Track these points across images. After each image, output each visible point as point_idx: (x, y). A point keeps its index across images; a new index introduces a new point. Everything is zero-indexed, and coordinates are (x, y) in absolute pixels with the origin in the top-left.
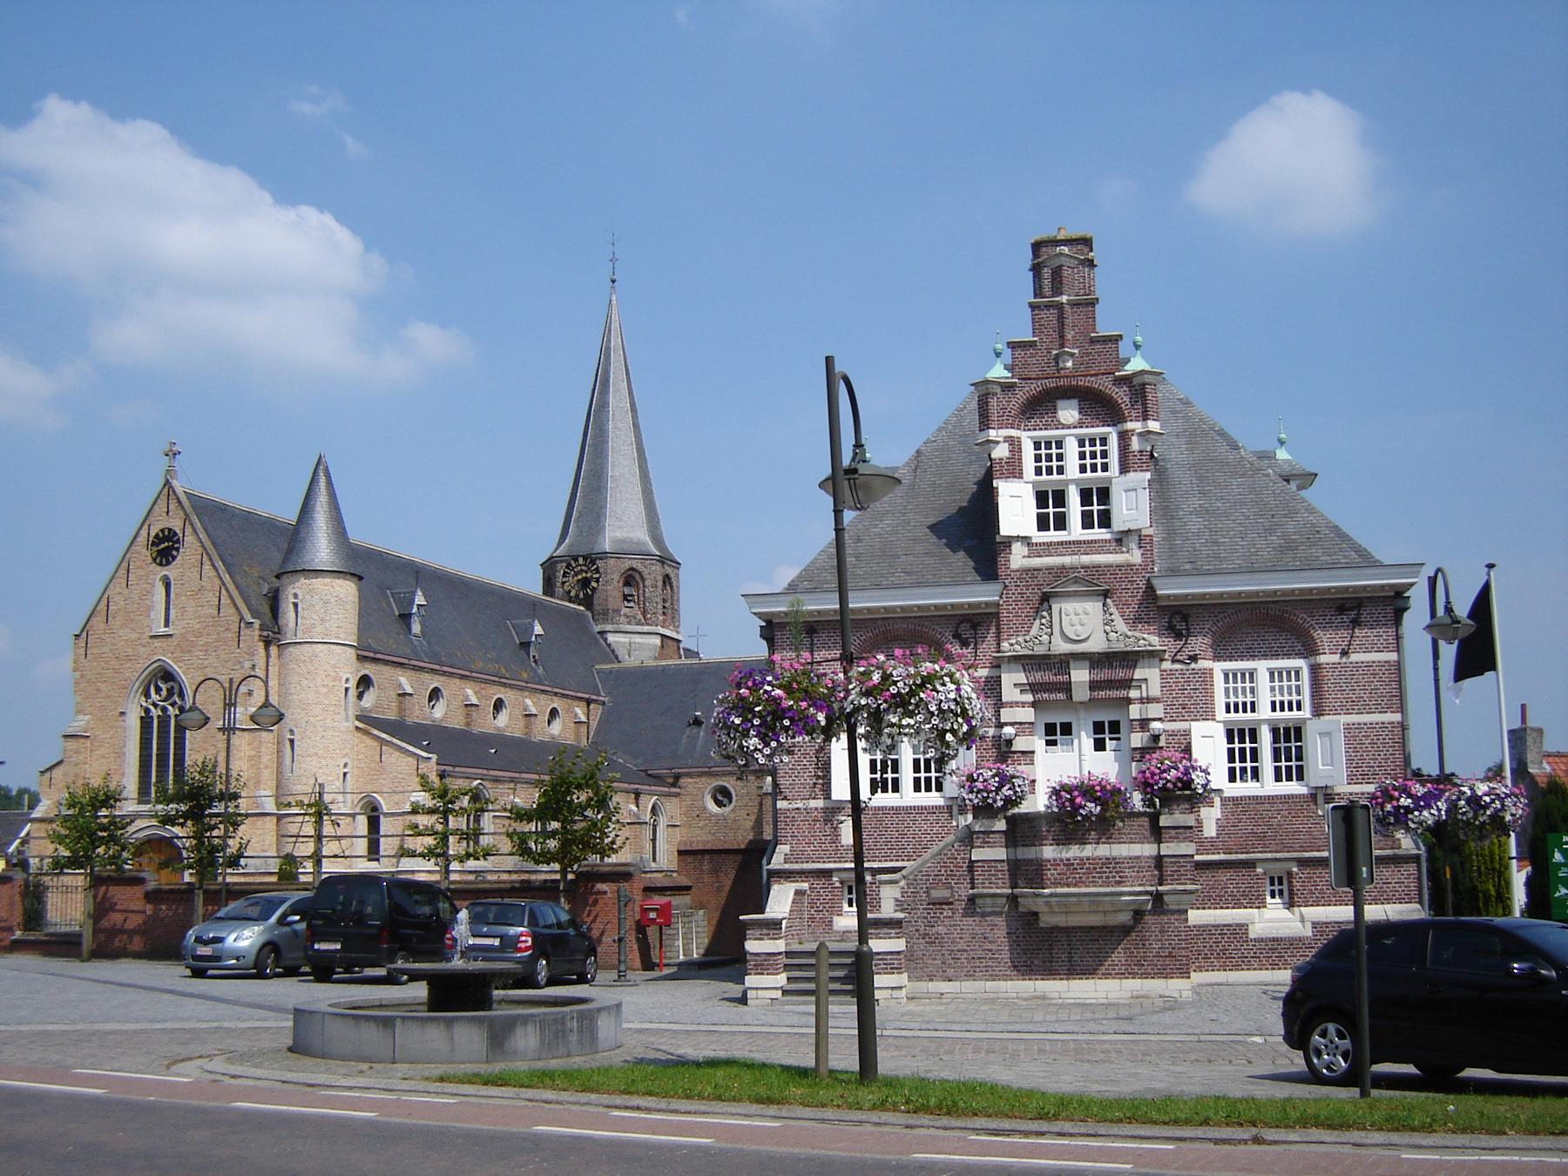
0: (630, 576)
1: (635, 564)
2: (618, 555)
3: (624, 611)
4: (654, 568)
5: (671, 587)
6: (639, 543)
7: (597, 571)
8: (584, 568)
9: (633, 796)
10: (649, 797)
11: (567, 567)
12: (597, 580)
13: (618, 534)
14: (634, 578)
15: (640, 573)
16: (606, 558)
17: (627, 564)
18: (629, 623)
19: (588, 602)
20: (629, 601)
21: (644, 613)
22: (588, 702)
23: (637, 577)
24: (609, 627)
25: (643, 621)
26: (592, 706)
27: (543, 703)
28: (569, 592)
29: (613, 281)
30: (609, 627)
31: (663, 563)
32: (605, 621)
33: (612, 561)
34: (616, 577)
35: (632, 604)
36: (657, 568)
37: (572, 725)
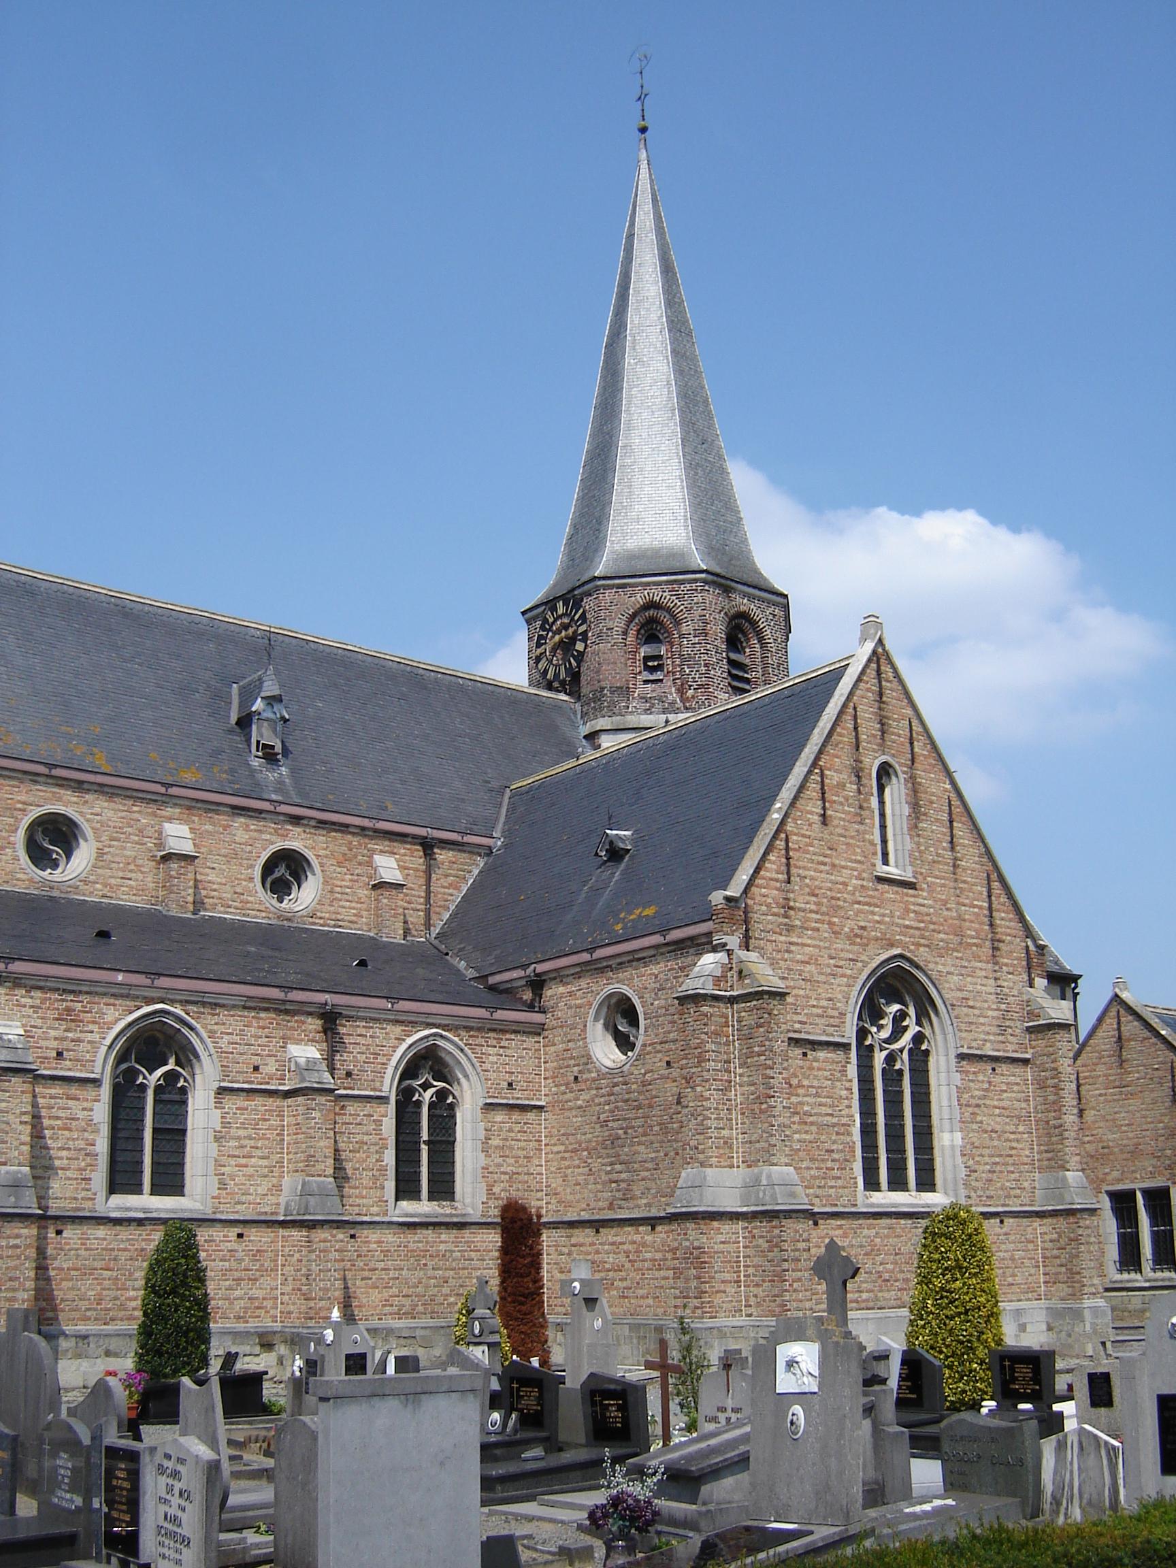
0: (652, 620)
1: (662, 595)
2: (620, 580)
3: (641, 689)
4: (698, 598)
5: (761, 640)
6: (673, 554)
7: (583, 618)
8: (566, 620)
9: (314, 1024)
10: (398, 1030)
11: (542, 628)
12: (585, 640)
13: (632, 543)
14: (661, 623)
15: (669, 610)
16: (597, 588)
17: (639, 599)
18: (648, 711)
19: (572, 683)
20: (652, 670)
21: (681, 691)
22: (428, 846)
23: (665, 618)
24: (602, 723)
25: (679, 704)
26: (442, 856)
27: (241, 836)
28: (546, 671)
29: (643, 130)
30: (602, 723)
31: (727, 590)
32: (598, 712)
33: (608, 596)
34: (618, 624)
35: (659, 675)
36: (711, 597)
37: (364, 893)
